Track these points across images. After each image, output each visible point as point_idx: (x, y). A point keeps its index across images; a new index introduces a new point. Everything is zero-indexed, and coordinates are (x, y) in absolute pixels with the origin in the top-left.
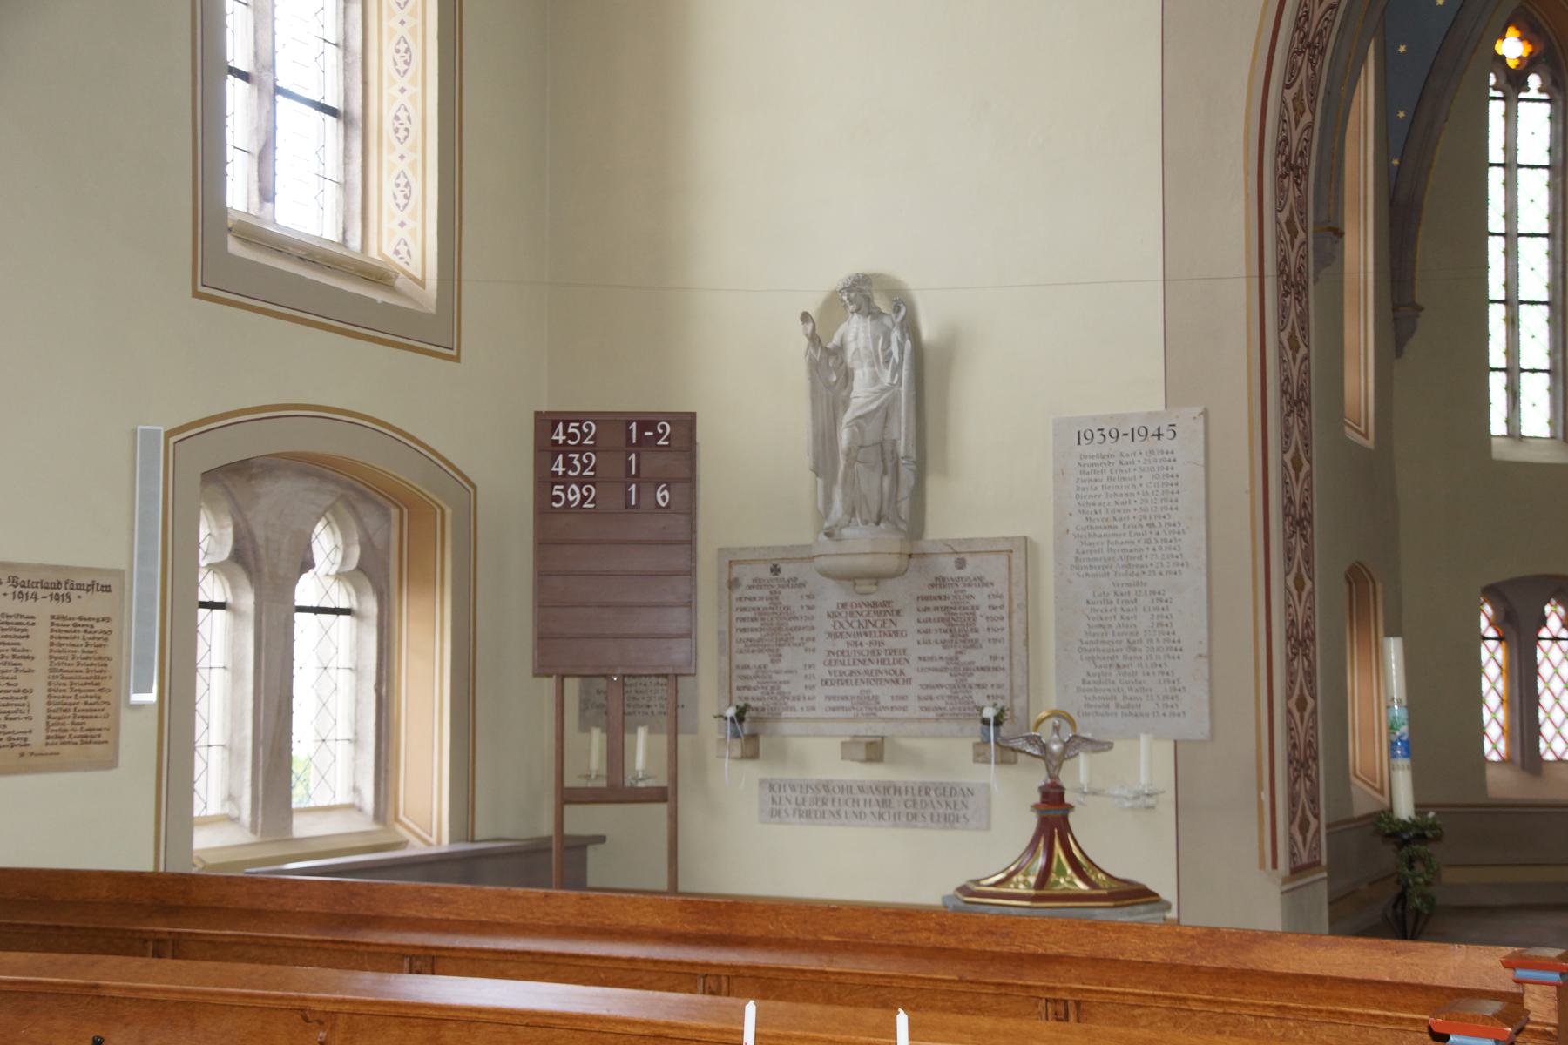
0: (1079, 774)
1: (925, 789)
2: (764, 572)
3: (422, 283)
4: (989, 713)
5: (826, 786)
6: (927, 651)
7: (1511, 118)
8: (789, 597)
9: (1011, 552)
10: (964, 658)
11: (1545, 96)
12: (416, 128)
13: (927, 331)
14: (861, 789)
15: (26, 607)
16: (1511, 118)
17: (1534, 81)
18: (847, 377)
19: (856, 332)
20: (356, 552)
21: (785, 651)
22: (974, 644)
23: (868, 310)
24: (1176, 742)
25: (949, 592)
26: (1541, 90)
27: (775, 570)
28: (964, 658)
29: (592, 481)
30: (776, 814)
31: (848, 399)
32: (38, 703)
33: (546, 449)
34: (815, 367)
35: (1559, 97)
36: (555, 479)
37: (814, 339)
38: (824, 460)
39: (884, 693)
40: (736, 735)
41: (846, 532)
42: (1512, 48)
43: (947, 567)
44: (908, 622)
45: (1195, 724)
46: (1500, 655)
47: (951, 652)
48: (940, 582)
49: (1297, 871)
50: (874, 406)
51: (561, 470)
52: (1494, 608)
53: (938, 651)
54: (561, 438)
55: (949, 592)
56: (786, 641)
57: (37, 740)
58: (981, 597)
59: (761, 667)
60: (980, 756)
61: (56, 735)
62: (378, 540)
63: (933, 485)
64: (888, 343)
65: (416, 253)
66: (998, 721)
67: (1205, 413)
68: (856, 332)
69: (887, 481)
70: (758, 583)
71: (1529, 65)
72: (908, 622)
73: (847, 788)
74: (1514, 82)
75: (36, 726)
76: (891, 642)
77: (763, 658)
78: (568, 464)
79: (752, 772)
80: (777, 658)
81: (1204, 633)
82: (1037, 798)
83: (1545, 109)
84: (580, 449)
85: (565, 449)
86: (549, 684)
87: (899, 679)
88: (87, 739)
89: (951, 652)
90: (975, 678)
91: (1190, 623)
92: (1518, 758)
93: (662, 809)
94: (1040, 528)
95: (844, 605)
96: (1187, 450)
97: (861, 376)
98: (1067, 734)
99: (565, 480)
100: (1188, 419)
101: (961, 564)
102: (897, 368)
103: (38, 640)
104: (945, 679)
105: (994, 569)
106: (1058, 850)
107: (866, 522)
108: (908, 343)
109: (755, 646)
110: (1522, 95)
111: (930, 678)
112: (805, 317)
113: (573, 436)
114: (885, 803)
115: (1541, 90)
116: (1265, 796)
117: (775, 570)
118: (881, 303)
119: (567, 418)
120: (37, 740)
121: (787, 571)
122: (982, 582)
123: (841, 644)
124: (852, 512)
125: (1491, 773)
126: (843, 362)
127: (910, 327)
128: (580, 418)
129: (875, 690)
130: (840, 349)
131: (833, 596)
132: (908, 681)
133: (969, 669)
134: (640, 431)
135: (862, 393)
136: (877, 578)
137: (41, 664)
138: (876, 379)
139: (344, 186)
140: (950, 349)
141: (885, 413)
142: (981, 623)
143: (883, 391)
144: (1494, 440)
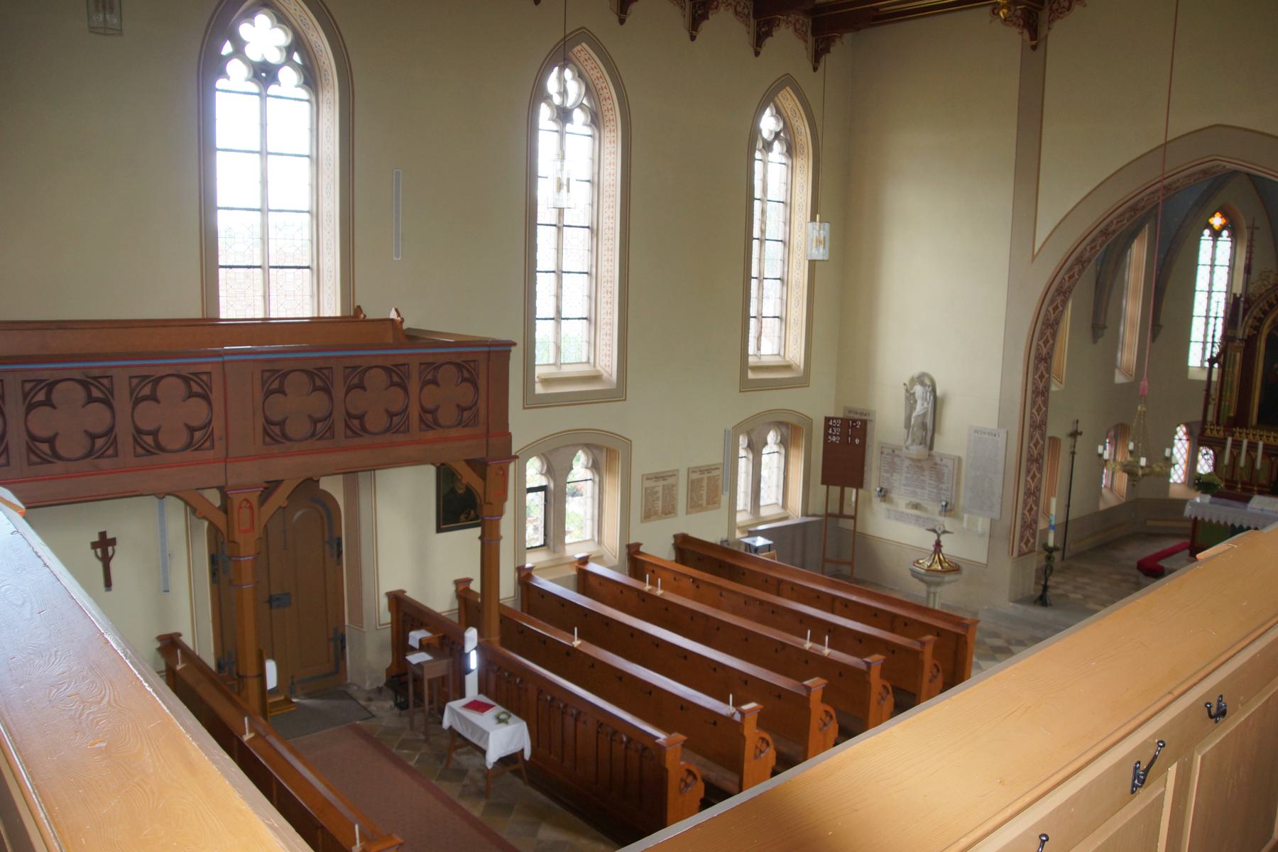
0: (943, 539)
1: (928, 519)
2: (891, 451)
3: (799, 367)
4: (944, 503)
5: (903, 513)
6: (931, 482)
7: (1214, 247)
8: (896, 459)
9: (954, 460)
10: (940, 486)
11: (1229, 239)
12: (799, 323)
13: (938, 393)
14: (912, 515)
15: (702, 476)
16: (1214, 247)
17: (1225, 233)
18: (916, 401)
19: (918, 389)
20: (779, 438)
21: (895, 474)
22: (942, 483)
23: (922, 384)
24: (992, 520)
25: (938, 467)
26: (1228, 237)
27: (893, 451)
28: (940, 486)
29: (839, 436)
30: (889, 518)
31: (915, 408)
32: (705, 497)
33: (827, 427)
34: (907, 398)
35: (1234, 240)
36: (829, 434)
37: (907, 391)
38: (908, 425)
39: (919, 491)
40: (879, 496)
41: (911, 448)
42: (1217, 221)
43: (938, 460)
44: (926, 473)
45: (996, 515)
46: (1186, 445)
47: (937, 484)
48: (936, 464)
49: (1021, 554)
50: (922, 412)
51: (830, 432)
52: (1186, 428)
53: (934, 483)
54: (831, 423)
55: (938, 467)
56: (895, 472)
57: (704, 504)
58: (946, 470)
59: (888, 478)
60: (940, 513)
61: (708, 503)
62: (785, 434)
63: (936, 436)
64: (926, 395)
65: (798, 358)
66: (946, 506)
67: (1007, 432)
68: (918, 389)
69: (924, 434)
70: (888, 454)
71: (1223, 227)
72: (926, 473)
73: (907, 514)
74: (1216, 235)
75: (704, 502)
76: (922, 478)
77: (888, 475)
78: (833, 431)
79: (884, 506)
80: (892, 476)
81: (1001, 491)
82: (934, 543)
83: (1229, 244)
84: (836, 427)
85: (832, 427)
86: (825, 487)
87: (923, 488)
88: (714, 503)
89: (937, 484)
90: (943, 492)
91: (998, 491)
92: (1187, 482)
93: (852, 521)
94: (962, 453)
95: (910, 465)
96: (1001, 440)
97: (919, 403)
98: (942, 529)
99: (832, 435)
100: (1003, 435)
101: (941, 460)
102: (928, 403)
103: (705, 483)
104: (935, 490)
105: (950, 463)
106: (937, 557)
107: (917, 444)
108: (932, 398)
109: (887, 471)
110: (1220, 239)
111: (931, 490)
112: (905, 384)
113: (833, 423)
114: (917, 520)
115: (1228, 237)
116: (1012, 537)
117: (893, 451)
118: (927, 382)
119: (833, 419)
120: (704, 504)
121: (896, 452)
122: (947, 466)
123: (909, 475)
124: (913, 441)
125: (1172, 488)
126: (914, 397)
127: (934, 390)
128: (837, 419)
129: (916, 490)
130: (914, 394)
131: (907, 463)
132: (926, 489)
133: (941, 489)
134: (852, 423)
135: (919, 409)
136: (919, 461)
137: (705, 488)
138: (923, 405)
139: (780, 338)
140: (943, 399)
141: (924, 415)
142: (946, 478)
143: (925, 408)
144: (1190, 369)
